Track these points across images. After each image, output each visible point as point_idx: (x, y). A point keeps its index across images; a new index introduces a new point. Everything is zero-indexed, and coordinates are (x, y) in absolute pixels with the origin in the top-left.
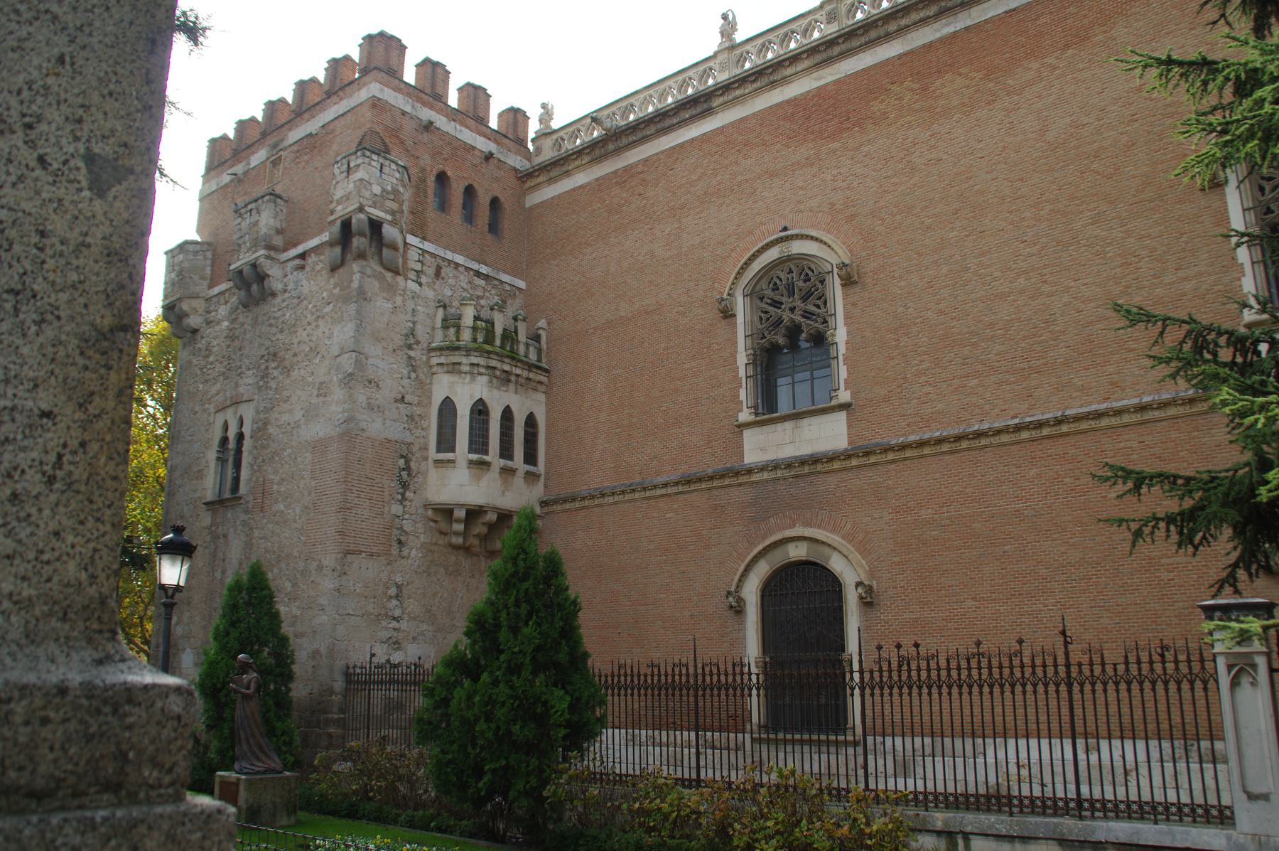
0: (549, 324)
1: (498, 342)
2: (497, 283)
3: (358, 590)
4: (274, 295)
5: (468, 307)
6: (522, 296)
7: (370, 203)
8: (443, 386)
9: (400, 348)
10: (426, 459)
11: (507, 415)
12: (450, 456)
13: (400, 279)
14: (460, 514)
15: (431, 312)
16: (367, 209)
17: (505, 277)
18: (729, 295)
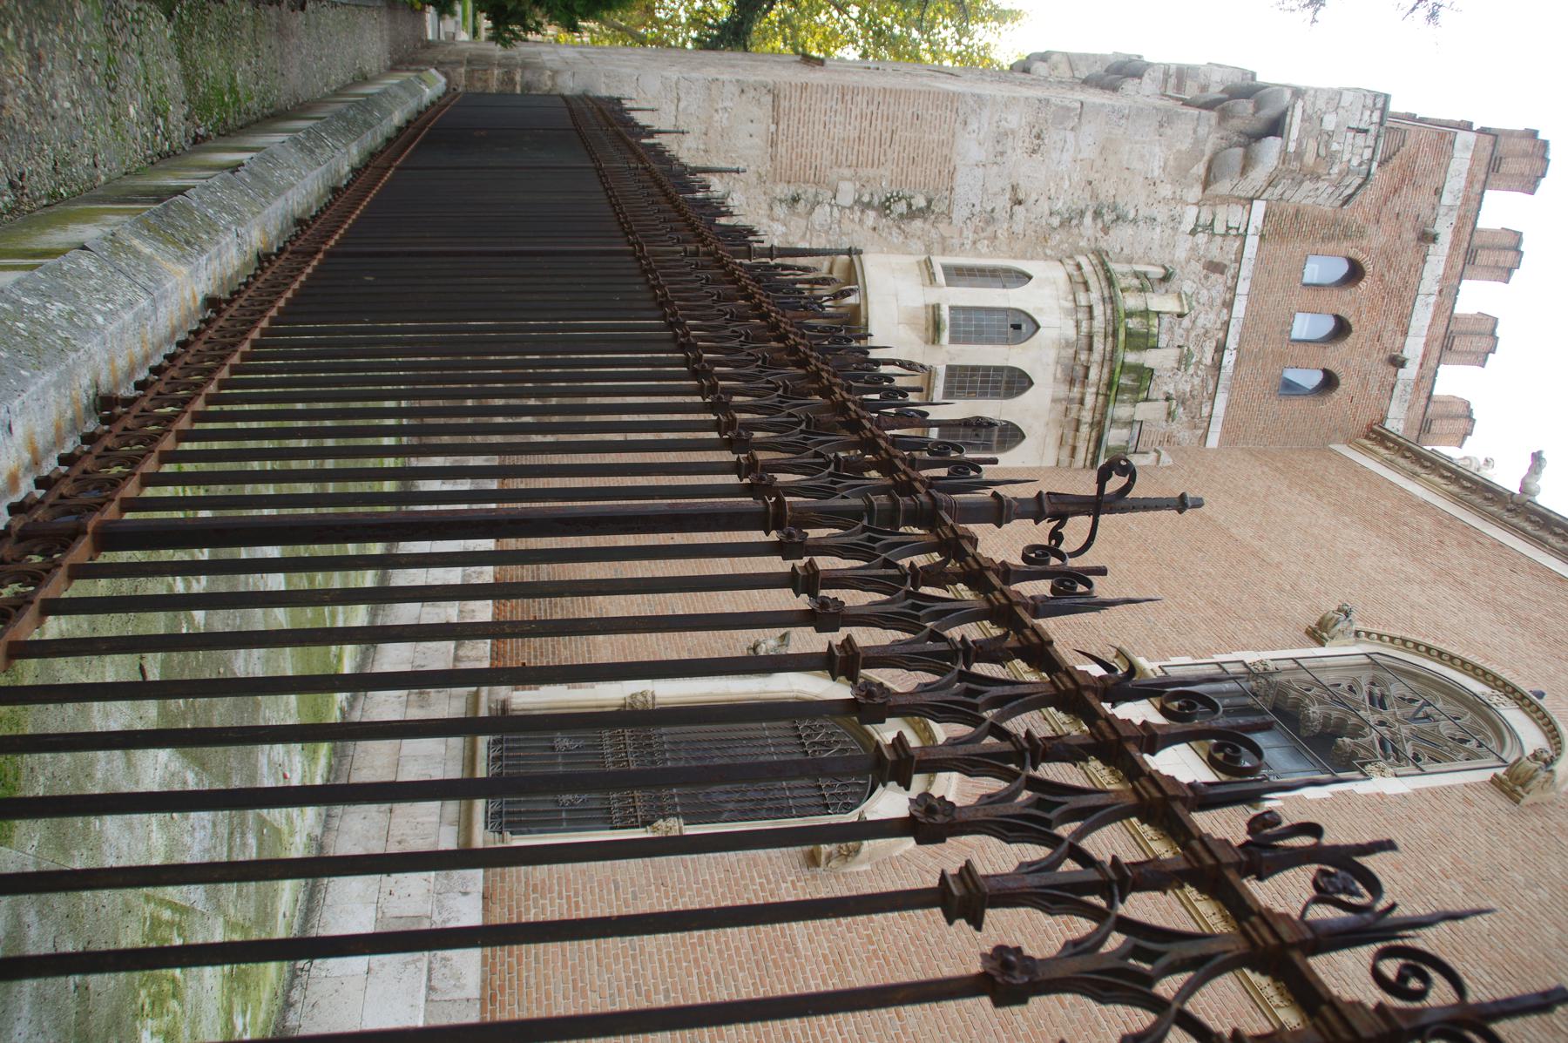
0: (1169, 468)
1: (1131, 358)
2: (1211, 388)
3: (717, 117)
6: (1195, 441)
7: (1309, 111)
9: (1094, 196)
11: (1015, 382)
12: (941, 278)
13: (1195, 193)
15: (1155, 255)
16: (1300, 103)
18: (1357, 633)
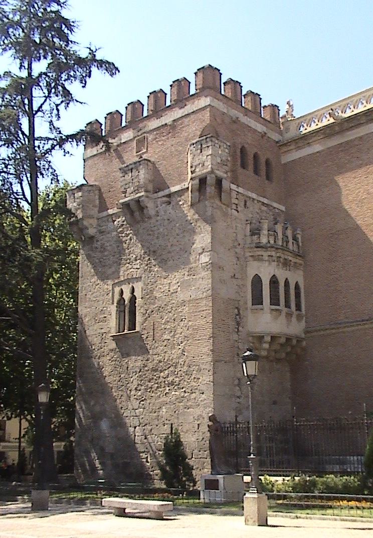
4: (150, 218)
8: (254, 268)
10: (247, 309)
11: (287, 283)
14: (268, 339)
17: (275, 205)
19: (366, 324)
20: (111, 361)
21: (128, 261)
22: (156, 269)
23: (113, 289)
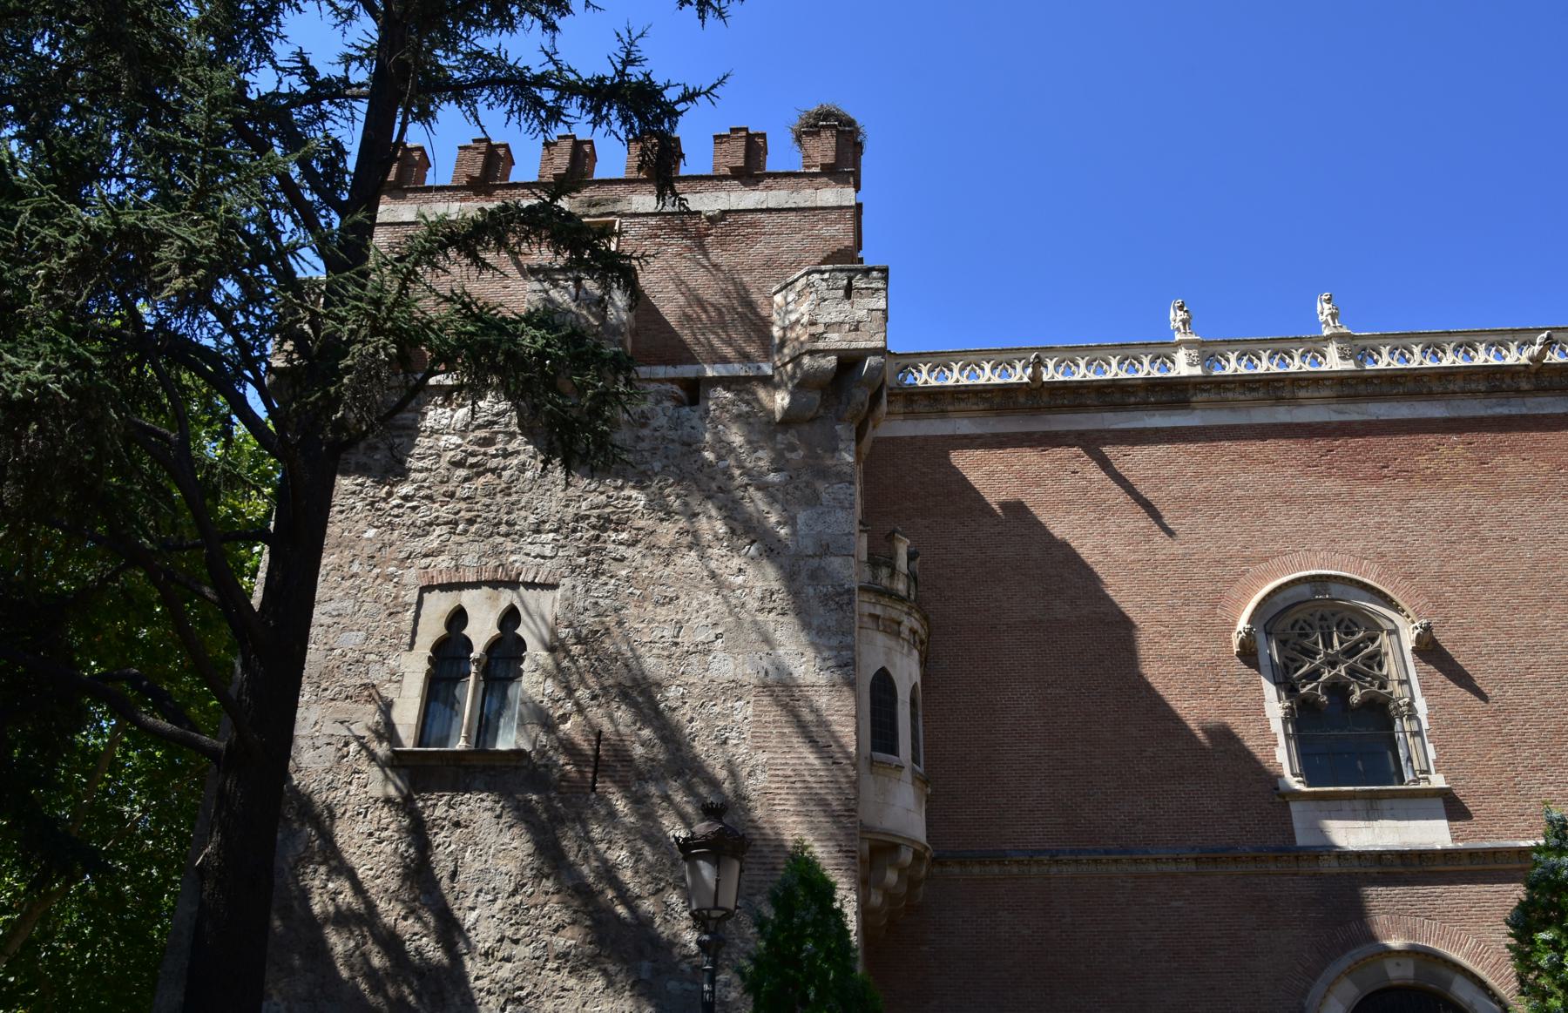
5: (902, 544)
19: (1116, 861)
20: (372, 840)
21: (503, 529)
22: (624, 573)
23: (420, 603)
